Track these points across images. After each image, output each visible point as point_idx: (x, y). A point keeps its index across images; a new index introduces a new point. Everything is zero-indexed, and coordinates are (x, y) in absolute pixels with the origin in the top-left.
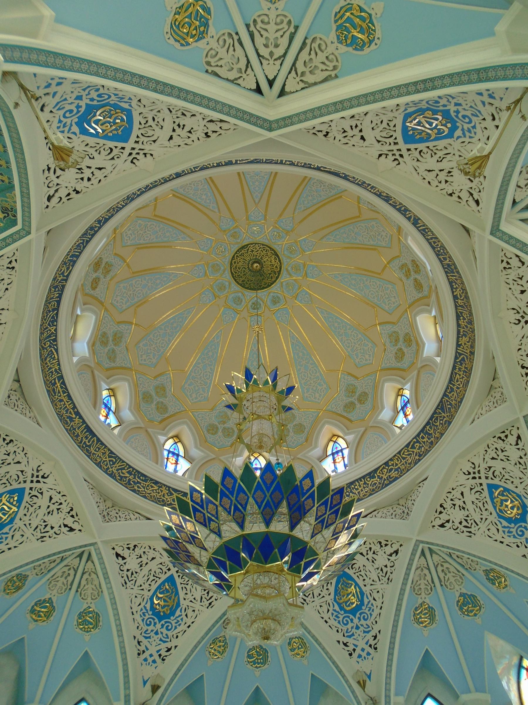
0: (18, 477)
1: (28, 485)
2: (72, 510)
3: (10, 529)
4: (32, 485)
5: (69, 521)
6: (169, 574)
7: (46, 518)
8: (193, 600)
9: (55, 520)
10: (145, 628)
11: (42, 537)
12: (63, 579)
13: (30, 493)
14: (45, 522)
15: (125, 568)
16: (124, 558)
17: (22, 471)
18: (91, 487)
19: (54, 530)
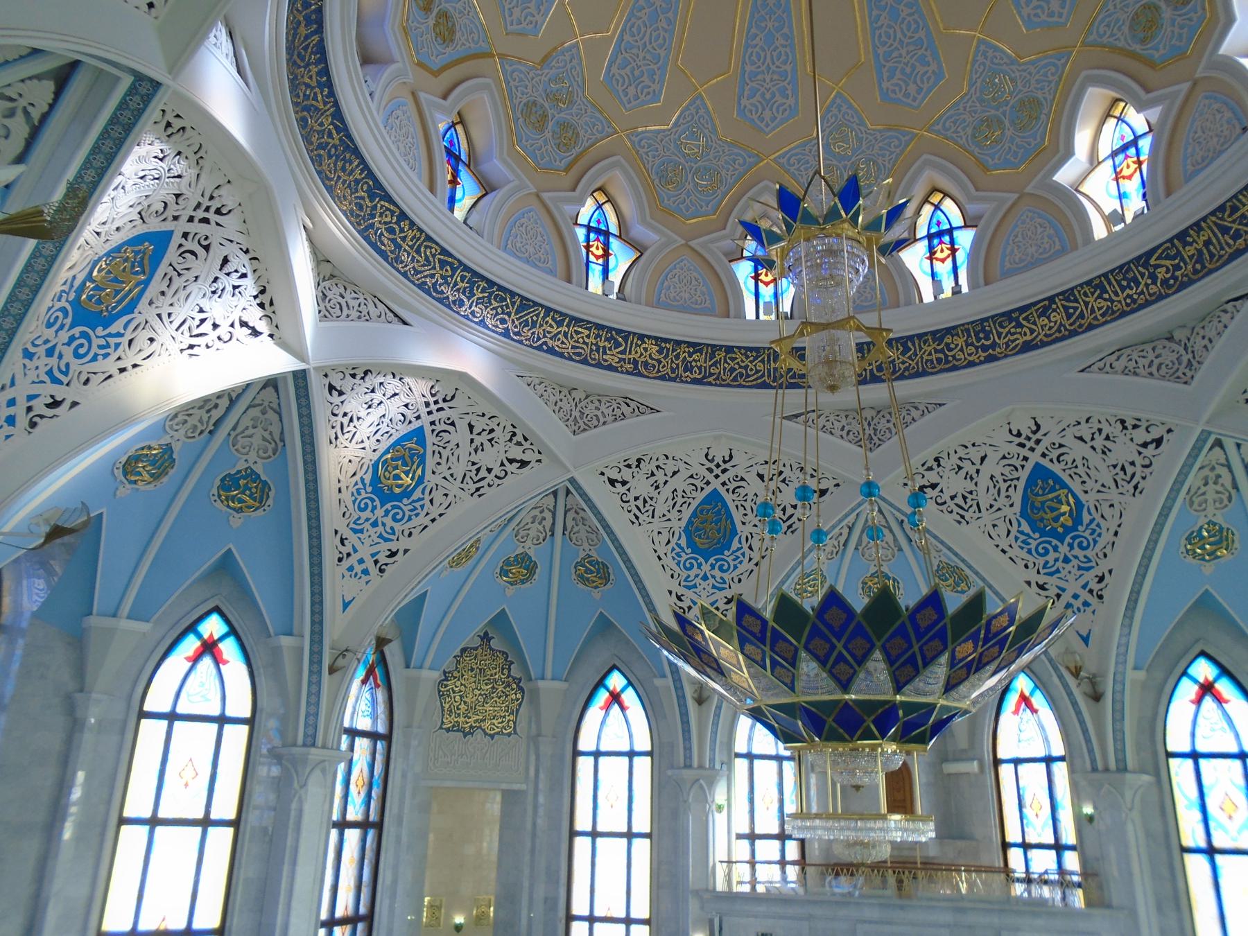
1: (426, 420)
2: (514, 434)
4: (431, 418)
5: (516, 453)
6: (708, 490)
7: (474, 458)
9: (491, 457)
10: (684, 574)
11: (478, 489)
14: (474, 464)
15: (631, 497)
16: (624, 483)
17: (406, 406)
18: (537, 381)
19: (493, 473)
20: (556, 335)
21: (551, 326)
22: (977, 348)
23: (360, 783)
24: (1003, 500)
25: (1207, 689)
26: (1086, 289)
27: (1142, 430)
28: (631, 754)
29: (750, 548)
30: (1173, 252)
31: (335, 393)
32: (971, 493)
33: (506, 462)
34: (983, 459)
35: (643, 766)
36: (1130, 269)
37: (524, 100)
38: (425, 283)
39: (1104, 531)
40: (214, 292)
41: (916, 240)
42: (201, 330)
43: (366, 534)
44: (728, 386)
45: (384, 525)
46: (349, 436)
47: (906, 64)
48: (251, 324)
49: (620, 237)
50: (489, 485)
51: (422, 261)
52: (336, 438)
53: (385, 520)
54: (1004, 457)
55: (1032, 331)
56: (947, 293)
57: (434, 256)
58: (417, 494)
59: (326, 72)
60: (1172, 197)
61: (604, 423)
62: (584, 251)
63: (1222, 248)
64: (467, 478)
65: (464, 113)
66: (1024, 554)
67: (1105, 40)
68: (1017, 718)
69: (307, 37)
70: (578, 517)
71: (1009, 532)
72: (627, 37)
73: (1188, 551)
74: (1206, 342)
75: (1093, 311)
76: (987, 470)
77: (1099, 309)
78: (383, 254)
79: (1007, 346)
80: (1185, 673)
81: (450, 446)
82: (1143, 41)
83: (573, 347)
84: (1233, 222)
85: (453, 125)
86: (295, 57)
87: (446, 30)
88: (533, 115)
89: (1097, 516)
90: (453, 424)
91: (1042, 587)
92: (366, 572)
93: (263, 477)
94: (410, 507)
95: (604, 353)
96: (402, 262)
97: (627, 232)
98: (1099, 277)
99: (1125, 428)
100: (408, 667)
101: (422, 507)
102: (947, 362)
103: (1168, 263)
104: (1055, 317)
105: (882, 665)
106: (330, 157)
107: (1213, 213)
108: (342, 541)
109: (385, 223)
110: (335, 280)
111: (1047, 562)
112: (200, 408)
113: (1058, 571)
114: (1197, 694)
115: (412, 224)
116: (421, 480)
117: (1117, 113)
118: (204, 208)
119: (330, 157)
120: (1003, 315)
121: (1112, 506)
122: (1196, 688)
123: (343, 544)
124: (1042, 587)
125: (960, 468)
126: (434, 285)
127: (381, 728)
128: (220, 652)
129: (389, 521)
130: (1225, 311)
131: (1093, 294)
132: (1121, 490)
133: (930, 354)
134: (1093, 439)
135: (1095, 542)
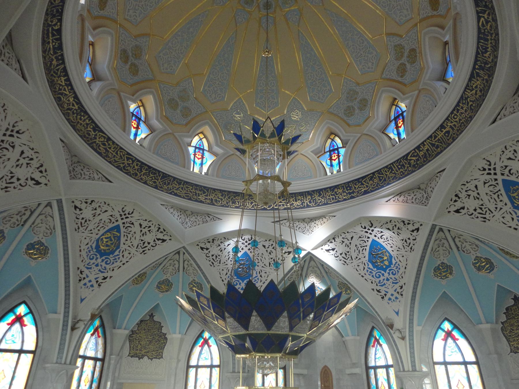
0: (110, 219)
2: (159, 228)
3: (119, 252)
4: (123, 221)
5: (160, 236)
7: (142, 238)
8: (264, 266)
9: (149, 238)
11: (144, 251)
12: (172, 267)
13: (124, 226)
14: (142, 240)
15: (210, 255)
16: (207, 249)
17: (111, 216)
19: (150, 245)
20: (178, 189)
21: (176, 185)
22: (347, 193)
23: (87, 381)
24: (361, 256)
25: (449, 334)
26: (386, 169)
27: (411, 225)
28: (211, 367)
29: (261, 276)
30: (416, 154)
31: (78, 210)
32: (348, 252)
33: (156, 240)
34: (352, 238)
35: (216, 372)
36: (401, 161)
37: (169, 98)
38: (120, 166)
39: (401, 267)
40: (17, 166)
41: (325, 153)
42: (12, 180)
43: (93, 270)
44: (250, 209)
45: (101, 266)
46: (85, 228)
47: (318, 87)
48: (36, 179)
49: (209, 151)
50: (149, 250)
51: (119, 157)
52: (79, 228)
53: (102, 264)
54: (360, 237)
55: (367, 186)
56: (335, 172)
57: (124, 155)
58: (117, 253)
59: (68, 80)
60: (413, 133)
61: (199, 224)
62: (192, 157)
63: (433, 152)
64: (139, 246)
65: (143, 101)
66: (370, 277)
67: (388, 77)
68: (374, 349)
69: (57, 65)
70: (189, 264)
71: (364, 268)
72: (211, 76)
73: (435, 275)
74: (432, 189)
75: (389, 178)
76: (354, 242)
77: (391, 177)
78: (100, 154)
79: (358, 192)
80: (439, 327)
81: (131, 233)
82: (402, 77)
83: (185, 193)
84: (436, 142)
85: (139, 107)
86: (52, 72)
87: (134, 70)
88: (172, 104)
89: (397, 260)
90: (133, 224)
91: (379, 291)
92: (92, 286)
93: (46, 245)
94: (113, 258)
95: (199, 196)
96: (109, 157)
97: (212, 149)
98: (390, 164)
99: (405, 224)
100: (115, 328)
101: (119, 258)
102: (336, 199)
103: (414, 158)
104: (376, 181)
105: (287, 320)
106: (73, 113)
107: (428, 138)
108: (81, 272)
109: (101, 141)
110: (80, 164)
111: (380, 281)
112: (17, 215)
113: (385, 284)
114: (445, 336)
115: (114, 142)
116: (118, 247)
117: (396, 104)
118: (10, 130)
119: (73, 113)
120: (355, 180)
121: (403, 256)
122: (444, 333)
123: (82, 274)
124: (379, 291)
125: (343, 242)
126: (124, 167)
127: (100, 356)
128: (23, 321)
129: (103, 264)
130: (437, 177)
131: (388, 171)
132: (406, 250)
133: (329, 196)
134: (393, 229)
135: (398, 272)
